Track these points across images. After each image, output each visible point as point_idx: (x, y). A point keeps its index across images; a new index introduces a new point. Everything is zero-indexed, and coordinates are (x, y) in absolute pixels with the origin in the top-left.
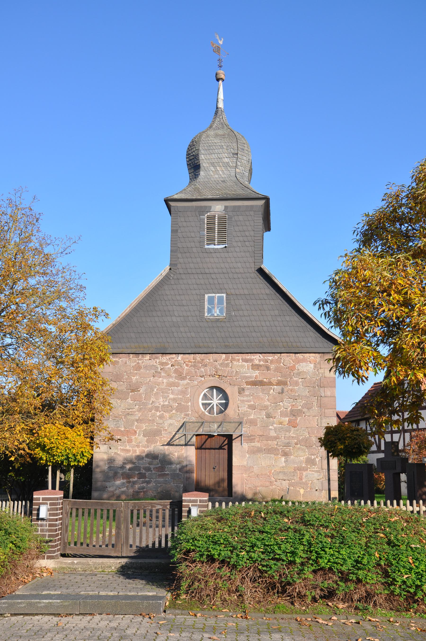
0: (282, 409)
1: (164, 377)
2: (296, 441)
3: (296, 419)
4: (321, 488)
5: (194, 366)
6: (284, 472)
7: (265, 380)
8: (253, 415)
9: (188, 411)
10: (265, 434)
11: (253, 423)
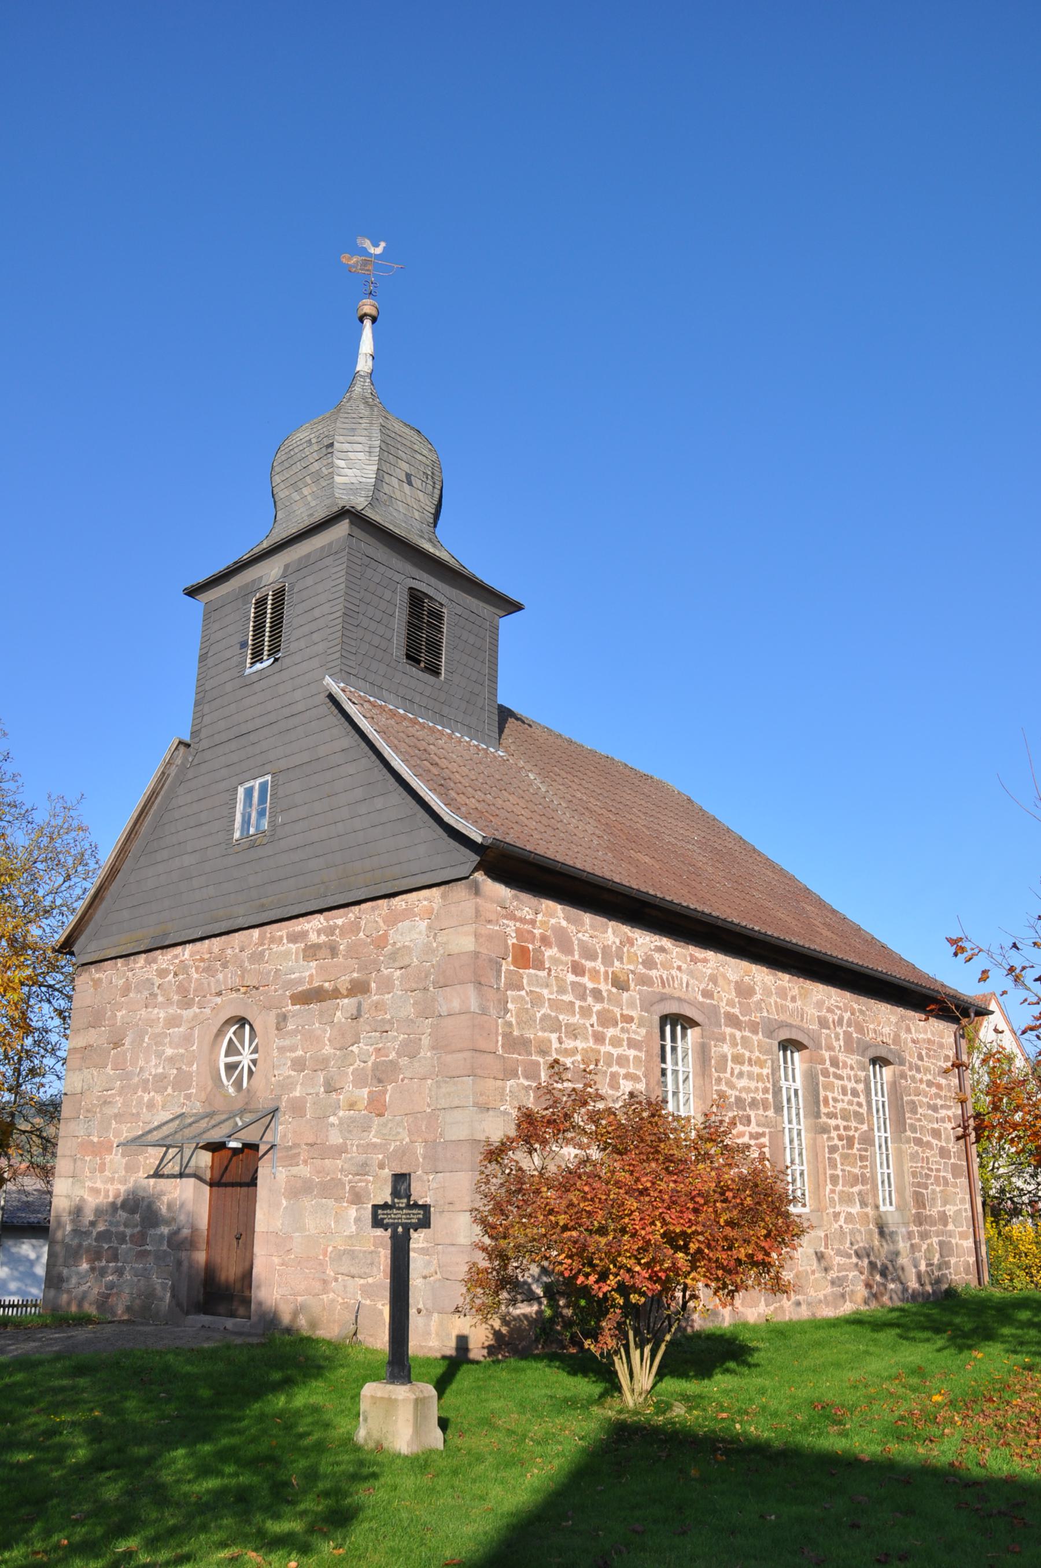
0: (356, 1066)
1: (161, 1006)
2: (380, 1156)
3: (385, 1092)
4: (429, 1306)
5: (207, 970)
6: (353, 1251)
7: (327, 985)
8: (299, 1087)
9: (189, 1088)
10: (318, 1142)
11: (298, 1108)
